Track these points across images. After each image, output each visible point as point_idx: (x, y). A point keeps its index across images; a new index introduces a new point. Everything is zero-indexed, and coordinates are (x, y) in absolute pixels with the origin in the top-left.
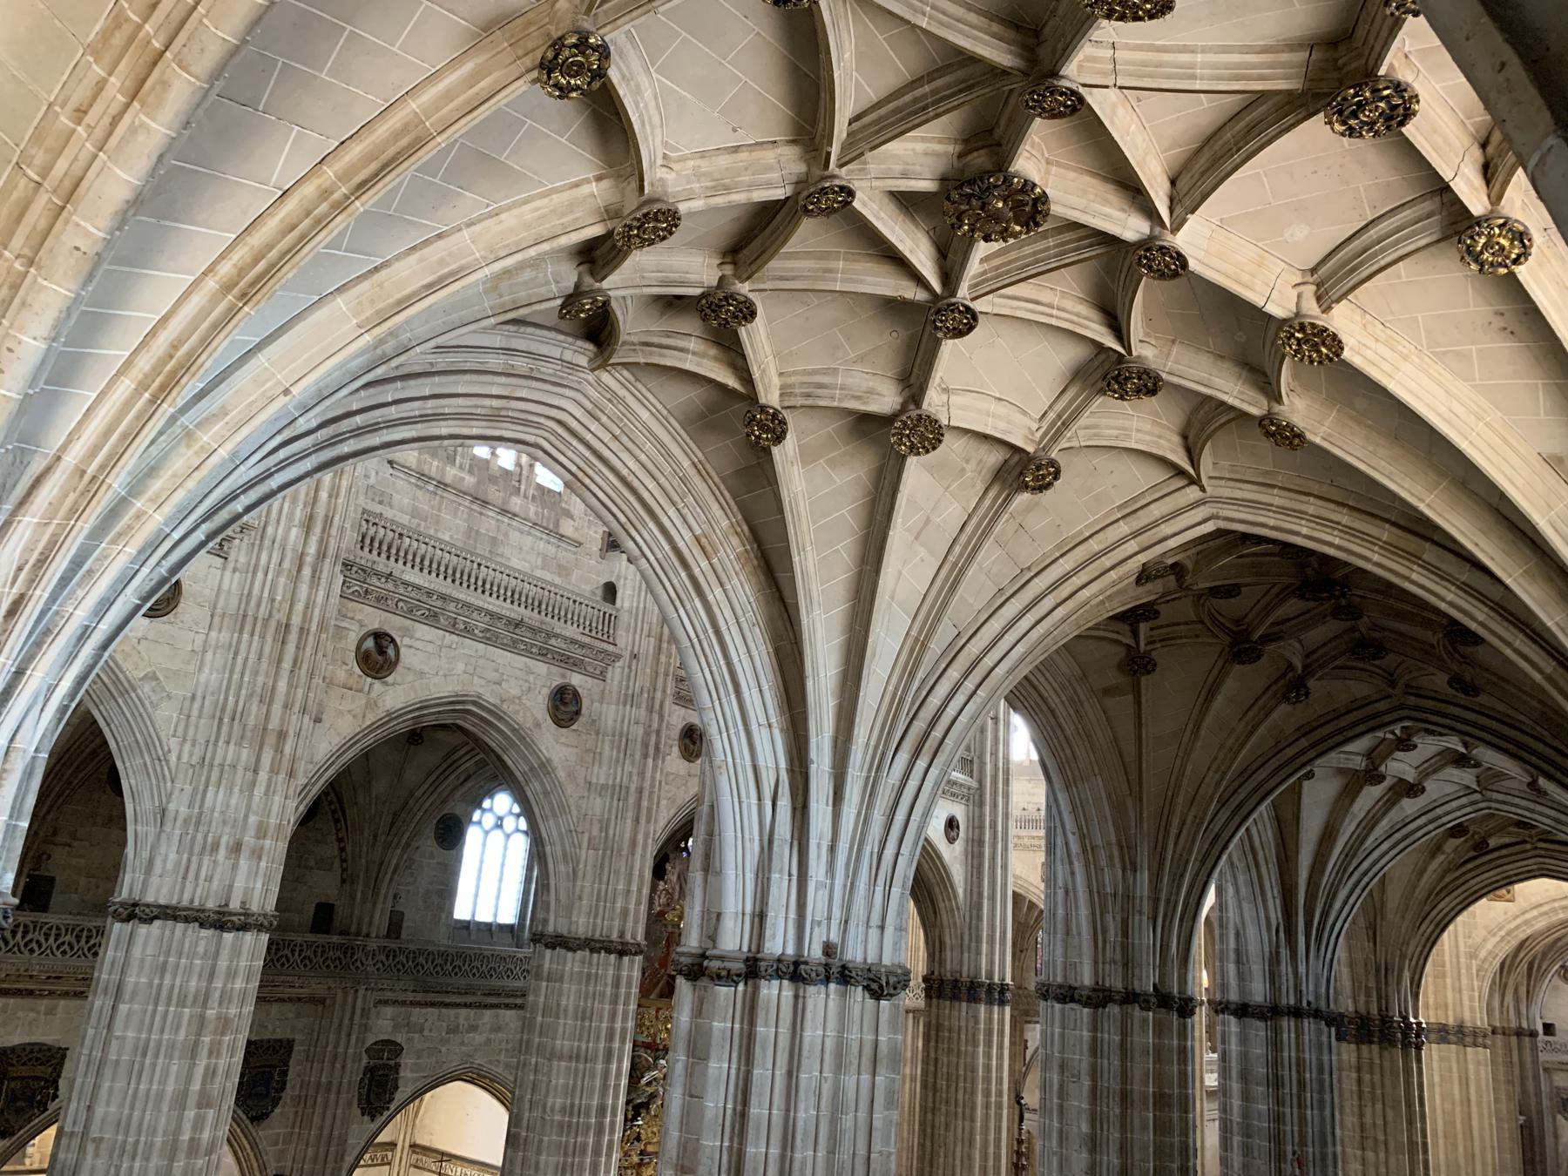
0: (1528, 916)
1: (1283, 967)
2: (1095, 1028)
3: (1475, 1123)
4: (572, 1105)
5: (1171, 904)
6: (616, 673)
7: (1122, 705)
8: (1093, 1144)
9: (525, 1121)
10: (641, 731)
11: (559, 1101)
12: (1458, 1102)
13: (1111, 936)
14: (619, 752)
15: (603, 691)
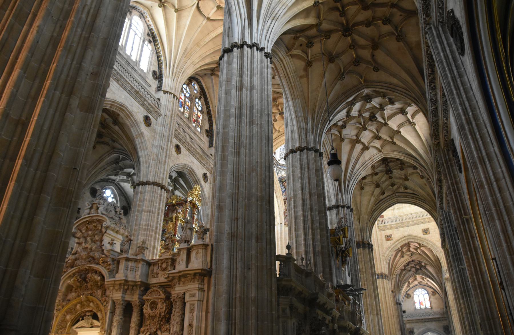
0: (396, 243)
1: (339, 196)
2: (300, 155)
3: (387, 298)
4: (148, 224)
5: (316, 131)
6: (160, 119)
7: (304, 80)
8: (302, 178)
9: (133, 229)
10: (167, 134)
11: (145, 218)
12: (382, 294)
13: (303, 137)
14: (161, 137)
15: (156, 123)
